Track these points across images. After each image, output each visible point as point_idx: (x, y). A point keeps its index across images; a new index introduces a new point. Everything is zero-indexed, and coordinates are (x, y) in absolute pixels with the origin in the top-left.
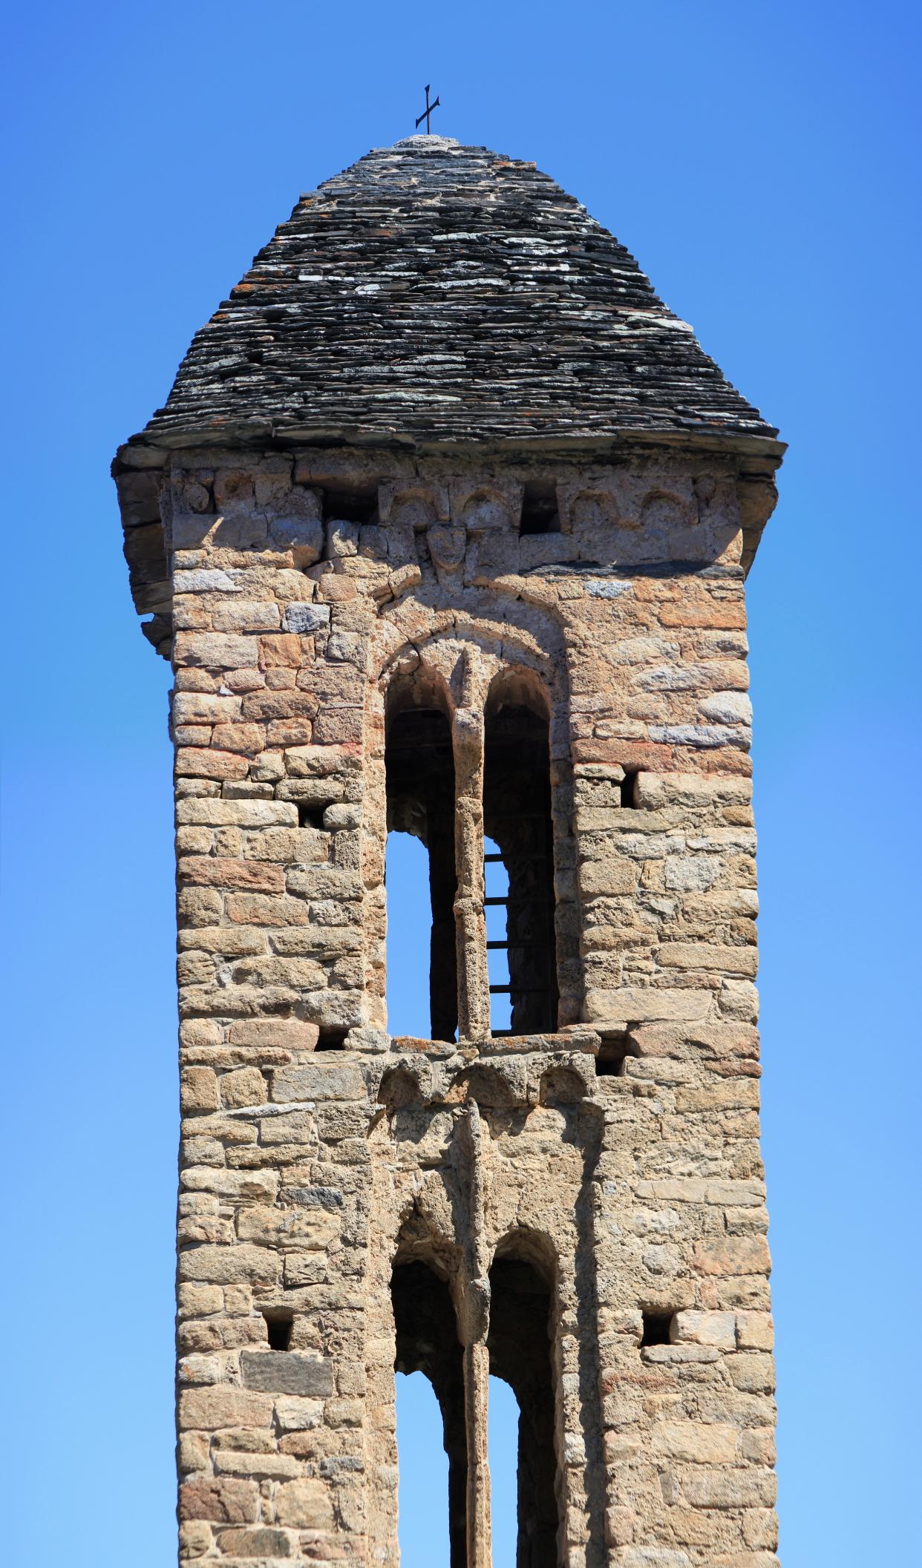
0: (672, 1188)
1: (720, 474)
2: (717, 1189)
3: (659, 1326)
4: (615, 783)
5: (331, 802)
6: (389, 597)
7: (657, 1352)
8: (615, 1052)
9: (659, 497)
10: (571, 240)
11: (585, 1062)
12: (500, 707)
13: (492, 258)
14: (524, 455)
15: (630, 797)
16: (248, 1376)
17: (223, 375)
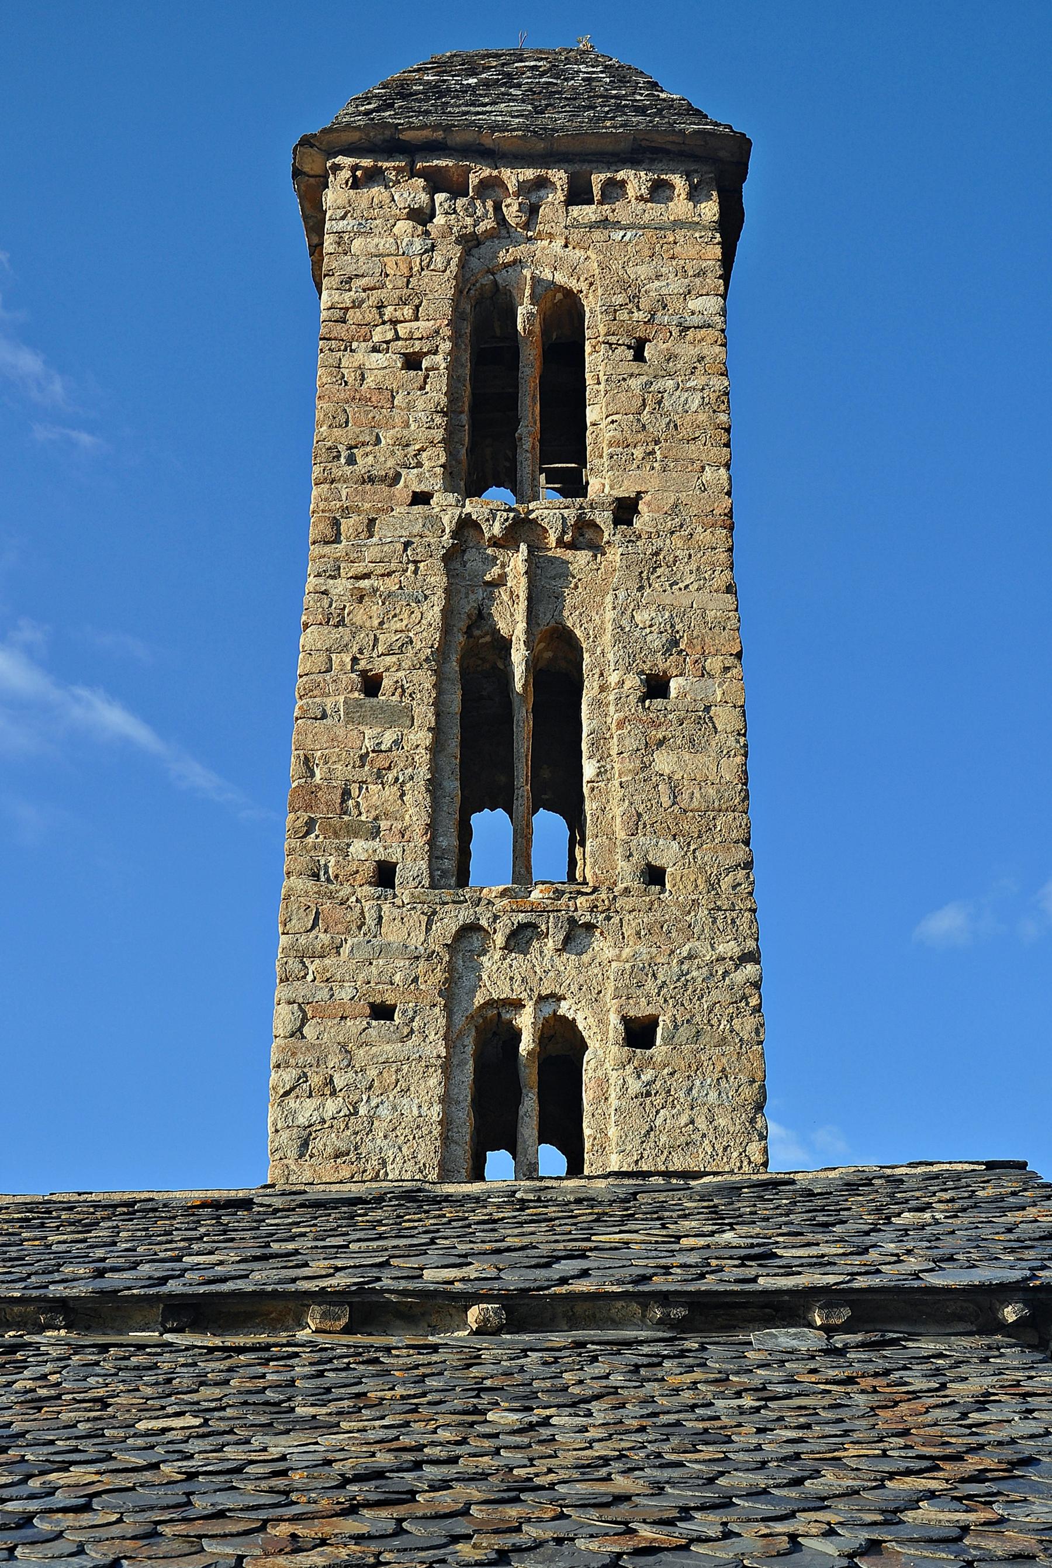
0: (667, 599)
1: (705, 168)
2: (699, 599)
3: (656, 687)
4: (629, 347)
5: (426, 354)
6: (475, 242)
7: (658, 703)
8: (625, 510)
9: (663, 186)
10: (606, 67)
11: (603, 518)
12: (554, 337)
13: (554, 70)
14: (570, 157)
15: (639, 357)
16: (346, 714)
17: (367, 113)
